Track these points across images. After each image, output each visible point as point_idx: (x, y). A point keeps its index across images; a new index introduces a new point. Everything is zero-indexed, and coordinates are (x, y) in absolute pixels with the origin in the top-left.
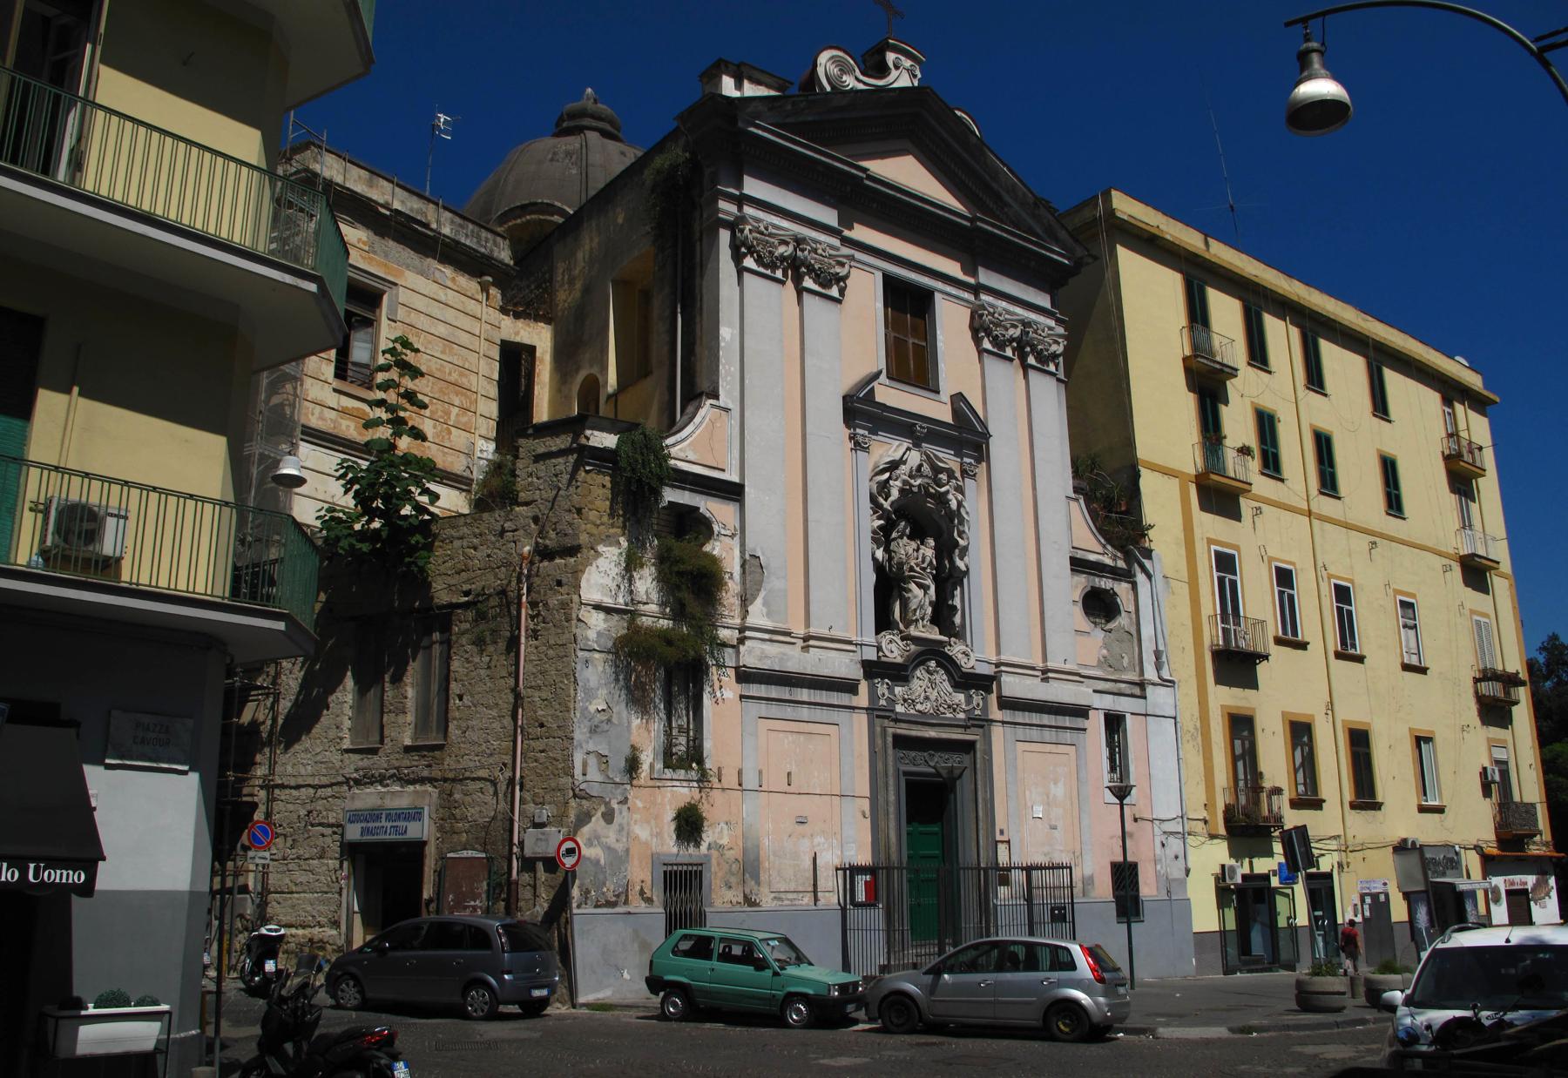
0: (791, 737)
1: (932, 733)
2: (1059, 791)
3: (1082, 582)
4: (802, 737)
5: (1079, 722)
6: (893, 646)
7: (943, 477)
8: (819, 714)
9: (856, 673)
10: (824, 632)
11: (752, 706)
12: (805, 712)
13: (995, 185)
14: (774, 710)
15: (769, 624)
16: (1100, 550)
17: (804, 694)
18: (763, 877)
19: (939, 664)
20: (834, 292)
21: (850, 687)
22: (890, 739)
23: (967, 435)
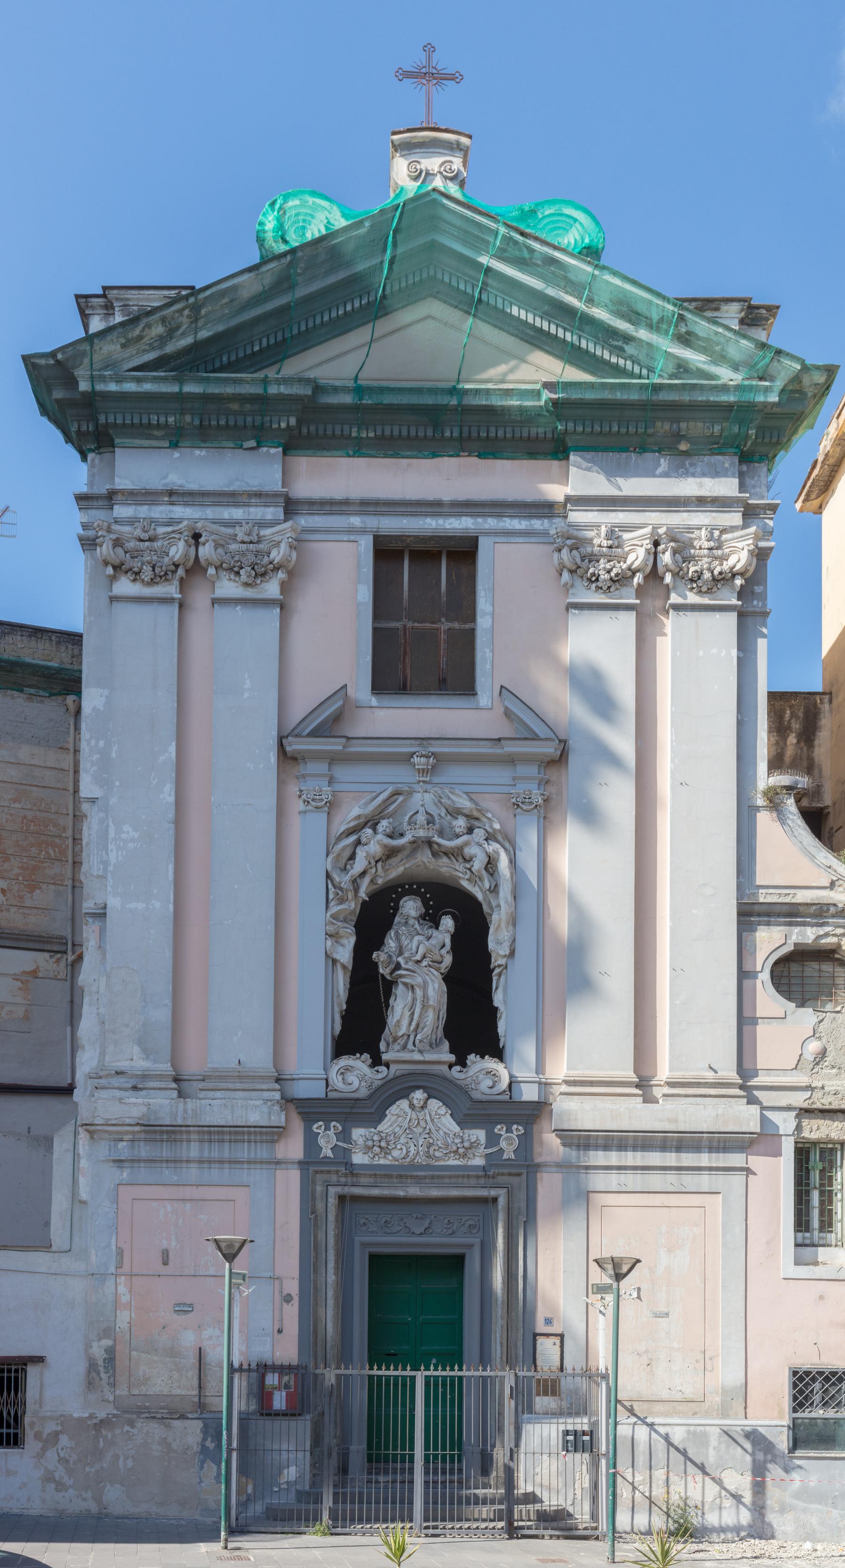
4: (188, 1206)
6: (352, 1078)
8: (215, 1173)
12: (193, 1172)
20: (272, 588)
21: (274, 1134)
22: (332, 1201)
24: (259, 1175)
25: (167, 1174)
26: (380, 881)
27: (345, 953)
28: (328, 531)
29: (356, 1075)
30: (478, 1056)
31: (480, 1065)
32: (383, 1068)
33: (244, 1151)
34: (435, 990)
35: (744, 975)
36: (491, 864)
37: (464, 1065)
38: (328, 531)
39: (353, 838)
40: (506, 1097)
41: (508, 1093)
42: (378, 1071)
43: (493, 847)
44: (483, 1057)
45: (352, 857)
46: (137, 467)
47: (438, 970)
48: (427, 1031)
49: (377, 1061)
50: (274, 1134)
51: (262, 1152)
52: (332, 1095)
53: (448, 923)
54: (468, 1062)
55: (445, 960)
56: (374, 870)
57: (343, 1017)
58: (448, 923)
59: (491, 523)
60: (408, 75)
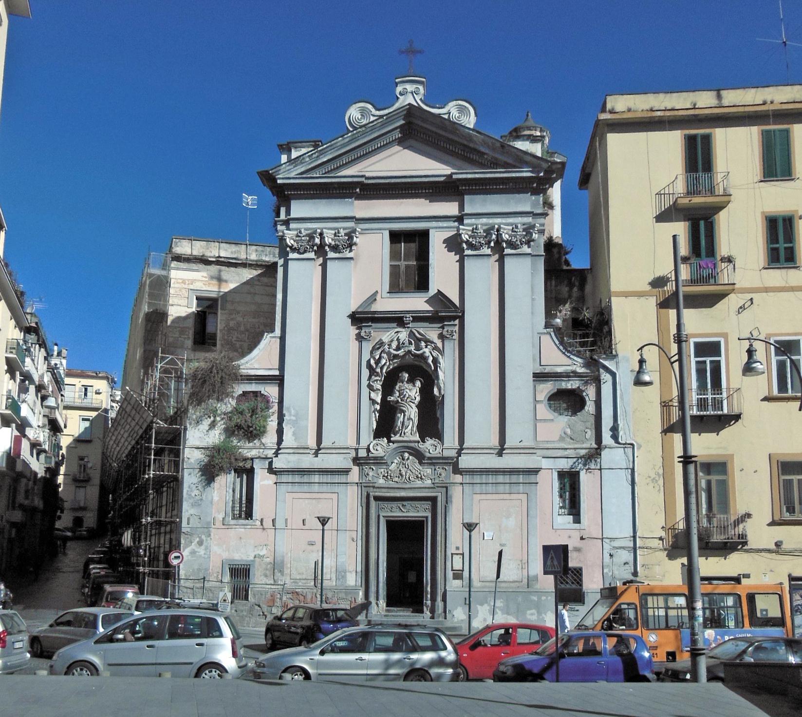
0: (307, 501)
1: (403, 494)
2: (511, 522)
3: (547, 388)
5: (532, 478)
6: (379, 448)
7: (423, 344)
8: (325, 488)
9: (349, 464)
10: (330, 445)
11: (283, 488)
12: (316, 488)
13: (471, 145)
14: (296, 488)
15: (295, 445)
16: (569, 362)
17: (316, 478)
18: (287, 571)
19: (410, 454)
21: (346, 472)
23: (447, 314)
24: (342, 487)
25: (306, 488)
27: (378, 398)
28: (372, 229)
29: (381, 448)
31: (430, 442)
33: (337, 479)
34: (413, 412)
35: (536, 401)
36: (435, 361)
37: (424, 442)
38: (372, 229)
39: (380, 350)
43: (435, 353)
45: (380, 358)
46: (299, 209)
48: (410, 427)
49: (389, 441)
50: (346, 472)
51: (343, 479)
52: (370, 455)
53: (418, 384)
57: (377, 423)
59: (434, 224)
60: (403, 52)
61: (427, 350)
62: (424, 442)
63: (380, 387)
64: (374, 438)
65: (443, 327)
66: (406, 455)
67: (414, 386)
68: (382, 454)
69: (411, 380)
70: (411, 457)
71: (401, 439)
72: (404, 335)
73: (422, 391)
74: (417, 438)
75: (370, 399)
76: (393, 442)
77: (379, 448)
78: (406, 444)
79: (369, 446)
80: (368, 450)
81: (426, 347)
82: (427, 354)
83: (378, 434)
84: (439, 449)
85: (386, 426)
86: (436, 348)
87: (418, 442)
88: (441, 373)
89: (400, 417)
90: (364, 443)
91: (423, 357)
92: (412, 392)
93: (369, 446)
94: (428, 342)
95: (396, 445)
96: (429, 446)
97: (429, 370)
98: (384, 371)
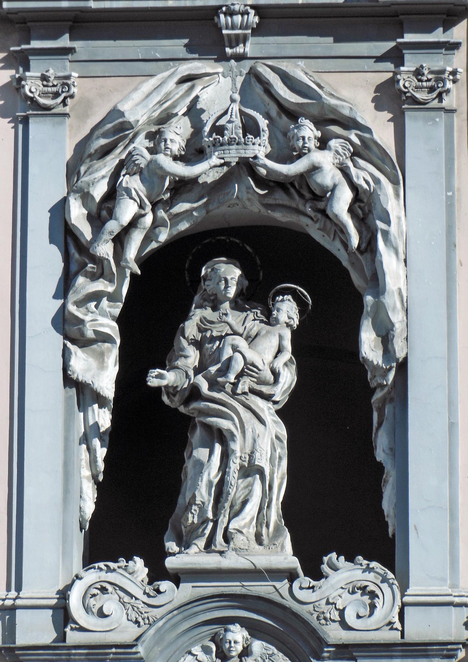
6: (110, 604)
19: (255, 630)
26: (163, 236)
30: (342, 558)
31: (344, 574)
32: (165, 585)
39: (111, 162)
40: (395, 637)
41: (398, 625)
42: (158, 591)
43: (364, 173)
44: (350, 559)
45: (112, 195)
47: (267, 398)
49: (158, 573)
52: (73, 637)
53: (287, 310)
54: (325, 568)
55: (282, 380)
56: (148, 220)
58: (287, 310)
61: (326, 160)
62: (315, 573)
63: (111, 328)
64: (89, 560)
65: (396, 57)
66: (237, 635)
67: (269, 319)
68: (127, 633)
69: (256, 296)
70: (257, 646)
71: (211, 561)
72: (218, 91)
73: (305, 345)
74: (285, 556)
75: (69, 381)
76: (176, 578)
77: (110, 604)
78: (234, 587)
79: (63, 595)
80: (62, 615)
81: (323, 144)
82: (330, 175)
83: (103, 542)
84: (386, 608)
85: (141, 494)
86: (366, 150)
87: (292, 576)
88: (390, 263)
89: (207, 462)
90: (41, 585)
91: (308, 191)
92: (265, 347)
93: (63, 595)
94: (330, 121)
95: (187, 591)
96: (342, 595)
97: (335, 247)
98: (132, 252)
